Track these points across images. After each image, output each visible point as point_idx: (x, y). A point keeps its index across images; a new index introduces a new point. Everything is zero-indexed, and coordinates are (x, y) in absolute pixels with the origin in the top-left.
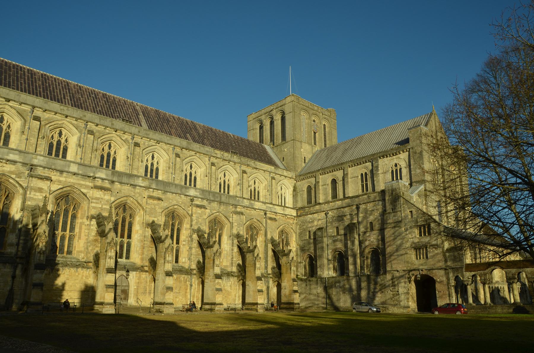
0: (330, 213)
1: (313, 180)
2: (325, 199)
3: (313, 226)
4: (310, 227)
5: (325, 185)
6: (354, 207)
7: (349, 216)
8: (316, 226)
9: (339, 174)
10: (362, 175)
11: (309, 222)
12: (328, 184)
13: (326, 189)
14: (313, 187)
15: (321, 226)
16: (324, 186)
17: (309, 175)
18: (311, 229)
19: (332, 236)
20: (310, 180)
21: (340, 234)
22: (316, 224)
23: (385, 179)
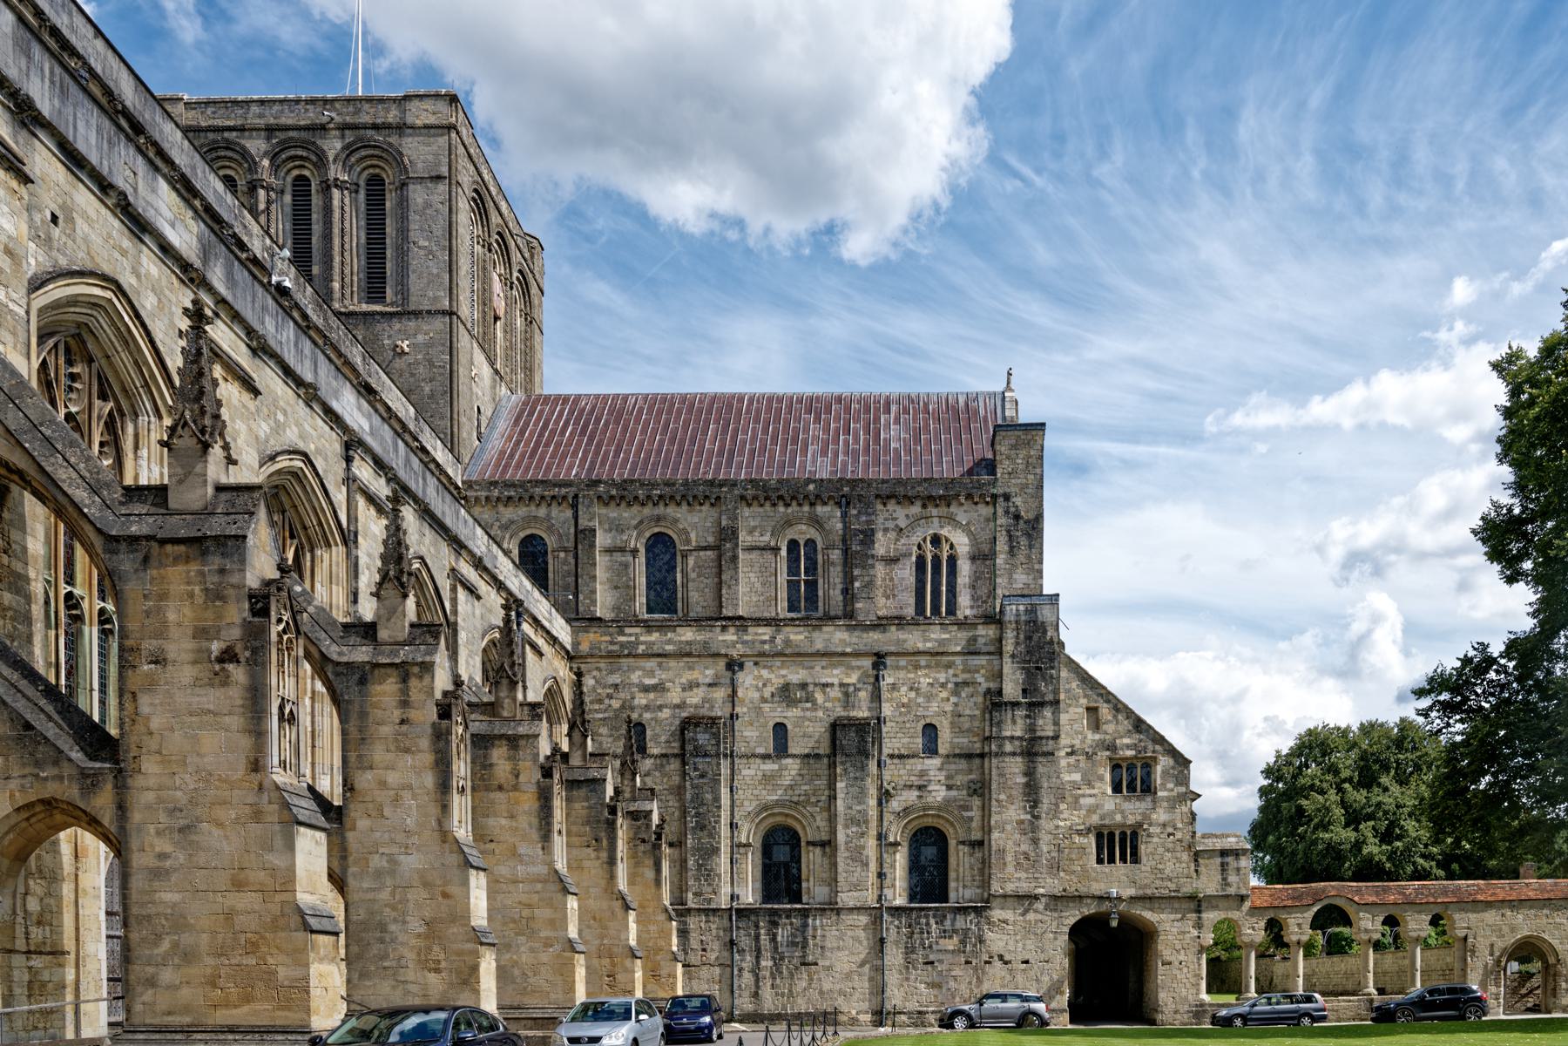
0: (749, 664)
1: (562, 515)
2: (617, 608)
3: (660, 708)
4: (647, 708)
5: (622, 550)
6: (867, 663)
7: (837, 688)
8: (677, 706)
9: (693, 525)
10: (793, 545)
11: (646, 689)
12: (635, 552)
13: (626, 566)
14: (551, 542)
15: (704, 712)
16: (618, 557)
17: (538, 491)
18: (647, 716)
19: (754, 756)
20: (542, 512)
21: (791, 751)
22: (677, 701)
23: (892, 580)
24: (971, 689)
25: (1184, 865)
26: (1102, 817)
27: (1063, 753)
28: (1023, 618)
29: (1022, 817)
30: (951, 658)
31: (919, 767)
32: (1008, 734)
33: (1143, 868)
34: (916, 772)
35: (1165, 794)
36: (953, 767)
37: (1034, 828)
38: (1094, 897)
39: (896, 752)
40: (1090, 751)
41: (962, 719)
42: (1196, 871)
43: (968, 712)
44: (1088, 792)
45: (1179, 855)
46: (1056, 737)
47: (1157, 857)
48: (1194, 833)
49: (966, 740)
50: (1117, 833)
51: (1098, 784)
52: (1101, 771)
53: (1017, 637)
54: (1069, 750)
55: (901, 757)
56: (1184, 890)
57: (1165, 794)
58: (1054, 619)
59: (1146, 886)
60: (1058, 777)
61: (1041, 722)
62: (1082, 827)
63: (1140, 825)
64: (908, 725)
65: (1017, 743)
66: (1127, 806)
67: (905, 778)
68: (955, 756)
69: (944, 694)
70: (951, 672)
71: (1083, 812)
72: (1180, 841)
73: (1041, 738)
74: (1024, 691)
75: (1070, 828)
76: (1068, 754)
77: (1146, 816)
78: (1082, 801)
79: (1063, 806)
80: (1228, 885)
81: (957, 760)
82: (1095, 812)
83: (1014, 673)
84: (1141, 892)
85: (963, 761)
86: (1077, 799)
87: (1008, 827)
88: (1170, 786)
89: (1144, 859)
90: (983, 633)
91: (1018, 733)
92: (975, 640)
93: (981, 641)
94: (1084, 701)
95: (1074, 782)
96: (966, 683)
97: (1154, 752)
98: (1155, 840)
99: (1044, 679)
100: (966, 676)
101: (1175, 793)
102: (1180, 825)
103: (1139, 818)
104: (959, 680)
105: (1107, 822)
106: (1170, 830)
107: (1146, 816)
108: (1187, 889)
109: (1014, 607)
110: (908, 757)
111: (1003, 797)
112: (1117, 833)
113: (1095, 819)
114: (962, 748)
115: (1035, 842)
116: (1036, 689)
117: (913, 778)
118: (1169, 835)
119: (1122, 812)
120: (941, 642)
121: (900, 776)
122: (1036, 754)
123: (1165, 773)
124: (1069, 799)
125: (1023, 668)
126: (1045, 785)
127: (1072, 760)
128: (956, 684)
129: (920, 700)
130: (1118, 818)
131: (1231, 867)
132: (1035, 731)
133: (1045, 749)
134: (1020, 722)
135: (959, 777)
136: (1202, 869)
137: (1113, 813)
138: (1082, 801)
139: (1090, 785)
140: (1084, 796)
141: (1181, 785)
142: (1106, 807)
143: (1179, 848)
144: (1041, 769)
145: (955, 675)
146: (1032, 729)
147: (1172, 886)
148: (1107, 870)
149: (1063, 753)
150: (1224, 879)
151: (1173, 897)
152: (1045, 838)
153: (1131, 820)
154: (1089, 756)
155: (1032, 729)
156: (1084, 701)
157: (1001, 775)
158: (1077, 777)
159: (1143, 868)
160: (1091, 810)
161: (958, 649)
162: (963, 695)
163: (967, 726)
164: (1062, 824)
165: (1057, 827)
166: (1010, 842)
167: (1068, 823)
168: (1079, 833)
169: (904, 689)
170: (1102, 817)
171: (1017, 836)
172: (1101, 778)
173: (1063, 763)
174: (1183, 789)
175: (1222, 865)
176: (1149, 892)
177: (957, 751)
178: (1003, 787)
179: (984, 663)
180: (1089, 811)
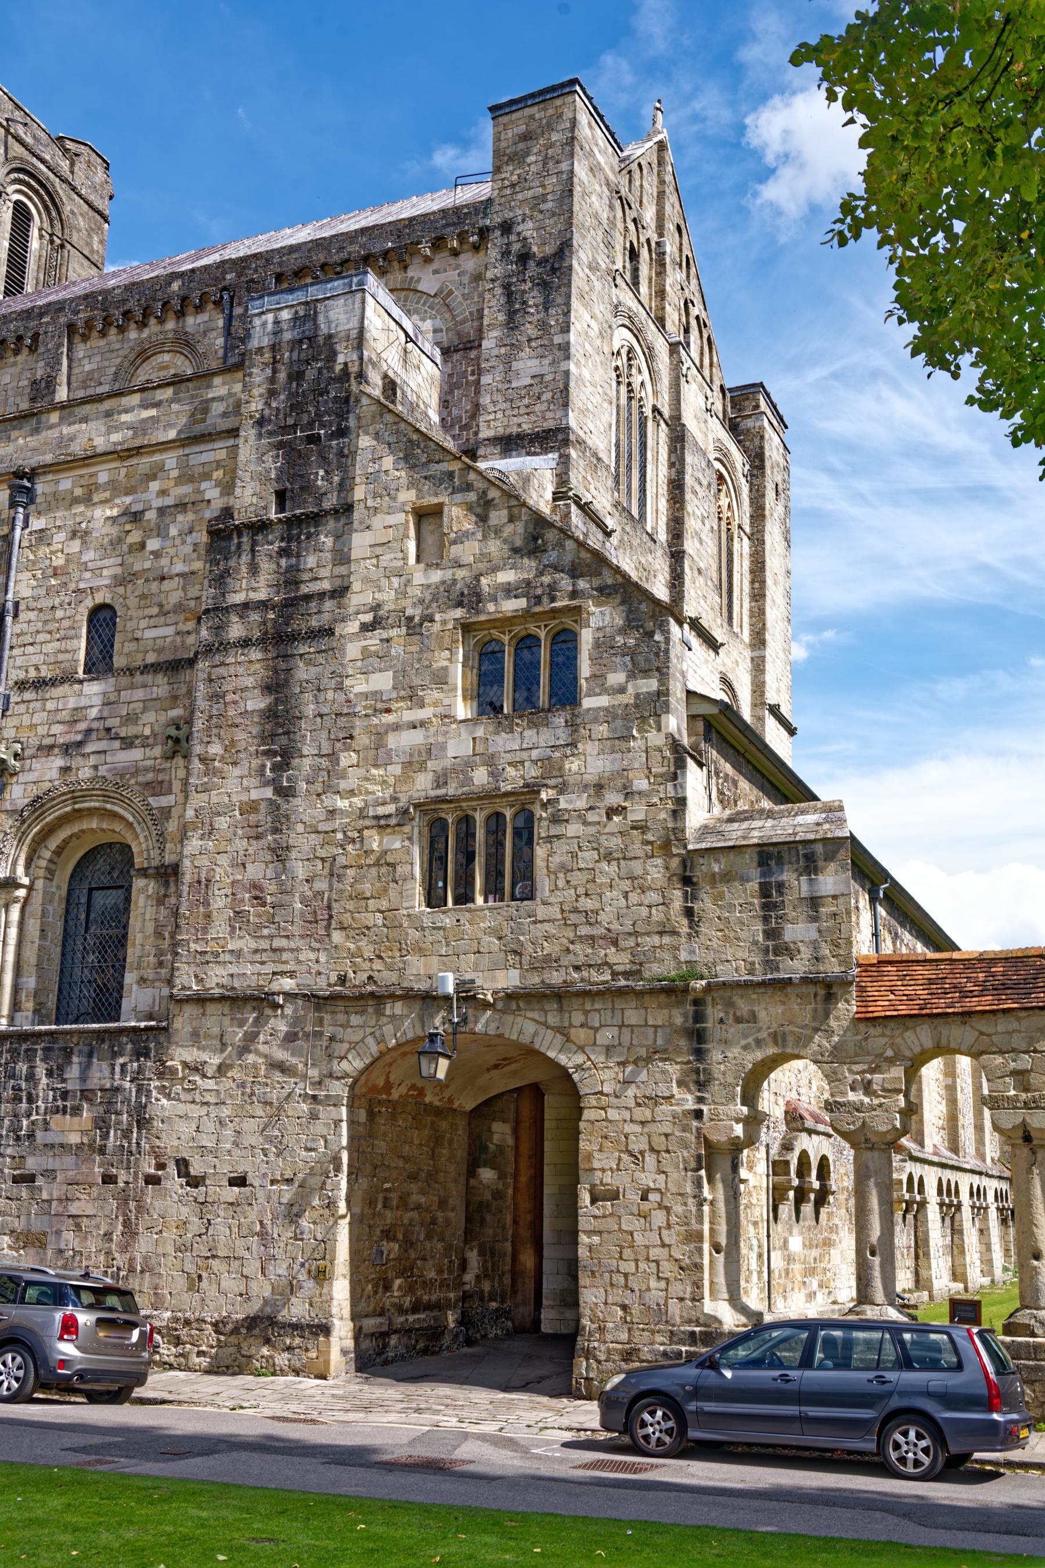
24: (190, 516)
25: (653, 897)
26: (441, 781)
27: (353, 627)
28: (287, 336)
29: (255, 795)
30: (157, 457)
31: (72, 703)
32: (238, 598)
33: (541, 912)
34: (65, 715)
35: (603, 701)
36: (139, 694)
37: (280, 821)
38: (409, 996)
39: (32, 674)
40: (416, 612)
41: (167, 585)
42: (689, 912)
43: (179, 567)
44: (409, 716)
45: (637, 867)
46: (340, 592)
47: (577, 878)
48: (681, 802)
49: (170, 631)
50: (479, 817)
51: (432, 695)
52: (441, 659)
53: (272, 380)
54: (368, 618)
55: (40, 684)
56: (654, 969)
57: (603, 701)
58: (354, 323)
59: (549, 962)
60: (340, 688)
61: (311, 561)
62: (391, 809)
63: (532, 789)
64: (59, 614)
65: (255, 616)
66: (504, 743)
67: (41, 730)
68: (147, 669)
69: (135, 537)
70: (155, 486)
71: (396, 769)
72: (641, 827)
73: (308, 598)
74: (281, 497)
75: (362, 814)
76: (365, 628)
77: (551, 768)
78: (393, 741)
79: (347, 759)
80: (787, 950)
81: (149, 678)
82: (422, 767)
83: (260, 460)
84: (534, 980)
85: (161, 679)
86: (379, 736)
87: (222, 823)
88: (616, 678)
89: (543, 884)
90: (223, 391)
91: (262, 595)
92: (206, 411)
93: (218, 408)
94: (407, 496)
95: (376, 694)
96: (181, 506)
97: (574, 594)
98: (573, 829)
99: (324, 460)
100: (179, 492)
101: (628, 698)
102: (641, 784)
103: (533, 772)
104: (169, 501)
105: (451, 790)
106: (613, 799)
107: (551, 768)
108: (662, 968)
109: (270, 317)
110: (53, 682)
111: (215, 749)
112: (479, 817)
113: (423, 785)
114: (159, 651)
115: (280, 854)
116: (307, 488)
117: (57, 729)
118: (611, 812)
119: (490, 761)
120: (140, 428)
121: (33, 727)
122: (294, 637)
123: (603, 645)
124: (363, 740)
125: (280, 445)
126: (310, 710)
127: (373, 641)
128: (161, 511)
129: (89, 556)
130: (480, 777)
131: (790, 897)
132: (297, 583)
133: (314, 623)
134: (266, 566)
135: (150, 717)
136: (706, 905)
137: (467, 765)
138: (393, 741)
139: (414, 699)
140: (397, 727)
141: (646, 673)
142: (451, 753)
143: (637, 849)
144: (303, 672)
145: (163, 493)
146: (290, 579)
147: (621, 960)
148: (448, 921)
149: (353, 627)
150: (772, 934)
151: (622, 992)
152: (301, 841)
153: (513, 779)
154: (413, 627)
155: (290, 579)
156: (407, 496)
157: (216, 697)
158: (383, 681)
159: (541, 912)
160: (414, 764)
161: (172, 434)
162: (173, 531)
163: (174, 598)
164: (341, 804)
165: (332, 813)
166: (223, 860)
167: (358, 802)
168: (381, 824)
169: (61, 536)
170: (441, 781)
171: (241, 844)
172: (441, 680)
173: (353, 650)
174: (651, 685)
175: (765, 891)
176: (556, 978)
177: (151, 658)
178: (218, 724)
179: (222, 455)
180: (408, 765)
